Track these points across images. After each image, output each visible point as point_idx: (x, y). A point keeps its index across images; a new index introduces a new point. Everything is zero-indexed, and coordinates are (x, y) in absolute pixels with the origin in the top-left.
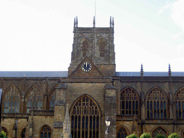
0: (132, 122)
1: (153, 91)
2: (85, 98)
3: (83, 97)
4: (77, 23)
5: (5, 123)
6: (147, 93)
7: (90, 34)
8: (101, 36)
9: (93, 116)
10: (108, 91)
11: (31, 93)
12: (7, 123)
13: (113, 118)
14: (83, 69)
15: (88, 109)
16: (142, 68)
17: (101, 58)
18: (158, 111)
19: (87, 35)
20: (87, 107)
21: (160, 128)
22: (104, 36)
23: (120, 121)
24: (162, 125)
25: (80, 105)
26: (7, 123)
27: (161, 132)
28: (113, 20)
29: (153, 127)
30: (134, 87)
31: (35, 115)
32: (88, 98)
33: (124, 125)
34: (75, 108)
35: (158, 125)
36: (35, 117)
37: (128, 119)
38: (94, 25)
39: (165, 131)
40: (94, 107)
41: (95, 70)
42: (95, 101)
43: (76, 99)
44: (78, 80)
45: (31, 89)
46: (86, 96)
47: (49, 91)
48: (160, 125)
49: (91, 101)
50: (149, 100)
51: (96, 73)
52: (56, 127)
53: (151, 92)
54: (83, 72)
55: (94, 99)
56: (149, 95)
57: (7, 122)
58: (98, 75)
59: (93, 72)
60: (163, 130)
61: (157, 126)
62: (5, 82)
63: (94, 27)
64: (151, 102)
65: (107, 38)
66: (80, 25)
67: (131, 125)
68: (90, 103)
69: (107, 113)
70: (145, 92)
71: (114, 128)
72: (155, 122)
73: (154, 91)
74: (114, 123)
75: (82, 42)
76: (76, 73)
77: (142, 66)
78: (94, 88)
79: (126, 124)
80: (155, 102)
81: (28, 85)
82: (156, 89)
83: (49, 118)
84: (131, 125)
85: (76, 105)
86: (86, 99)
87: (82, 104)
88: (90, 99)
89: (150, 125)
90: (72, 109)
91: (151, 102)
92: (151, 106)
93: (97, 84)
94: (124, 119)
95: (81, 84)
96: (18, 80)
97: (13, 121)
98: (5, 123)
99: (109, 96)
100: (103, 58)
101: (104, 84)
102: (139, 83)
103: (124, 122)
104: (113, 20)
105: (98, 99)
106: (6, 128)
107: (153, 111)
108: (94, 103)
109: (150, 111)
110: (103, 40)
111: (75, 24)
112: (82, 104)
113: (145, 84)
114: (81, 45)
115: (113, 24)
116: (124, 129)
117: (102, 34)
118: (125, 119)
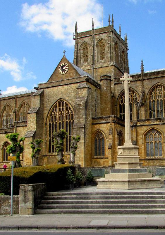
0: (109, 124)
1: (155, 89)
2: (61, 102)
3: (59, 102)
6: (148, 93)
7: (89, 38)
8: (100, 37)
9: (68, 121)
10: (80, 91)
13: (82, 122)
14: (60, 71)
15: (64, 114)
16: (142, 64)
17: (101, 60)
18: (162, 110)
19: (87, 40)
20: (63, 113)
21: (153, 130)
23: (97, 124)
24: (155, 126)
25: (56, 111)
27: (155, 134)
28: (112, 19)
29: (145, 129)
30: (133, 87)
31: (18, 127)
33: (101, 129)
34: (51, 114)
35: (151, 127)
36: (18, 128)
37: (105, 121)
38: (93, 27)
39: (160, 133)
40: (70, 112)
41: (71, 70)
42: (70, 104)
43: (52, 105)
44: (54, 84)
46: (61, 101)
48: (153, 126)
49: (67, 105)
50: (151, 99)
51: (72, 74)
52: (27, 136)
53: (153, 90)
54: (60, 75)
55: (69, 103)
56: (152, 93)
58: (75, 75)
59: (70, 73)
60: (158, 131)
61: (149, 128)
62: (18, 99)
63: (93, 29)
64: (154, 101)
65: (106, 39)
66: (79, 31)
67: (108, 128)
68: (66, 108)
69: (76, 115)
70: (147, 91)
71: (81, 132)
72: (148, 123)
73: (157, 88)
74: (82, 127)
75: (82, 48)
77: (142, 62)
78: (69, 91)
79: (103, 127)
80: (158, 100)
82: (159, 85)
84: (108, 128)
85: (53, 111)
86: (62, 104)
87: (58, 110)
88: (65, 102)
89: (142, 127)
90: (49, 117)
91: (154, 101)
92: (154, 106)
93: (72, 85)
94: (100, 122)
95: (57, 87)
96: (28, 96)
99: (81, 96)
100: (103, 61)
102: (139, 82)
103: (100, 125)
104: (112, 19)
105: (72, 102)
107: (156, 112)
108: (70, 107)
109: (152, 112)
110: (103, 41)
112: (58, 110)
113: (146, 82)
114: (82, 51)
115: (113, 22)
116: (101, 133)
117: (101, 35)
118: (102, 122)
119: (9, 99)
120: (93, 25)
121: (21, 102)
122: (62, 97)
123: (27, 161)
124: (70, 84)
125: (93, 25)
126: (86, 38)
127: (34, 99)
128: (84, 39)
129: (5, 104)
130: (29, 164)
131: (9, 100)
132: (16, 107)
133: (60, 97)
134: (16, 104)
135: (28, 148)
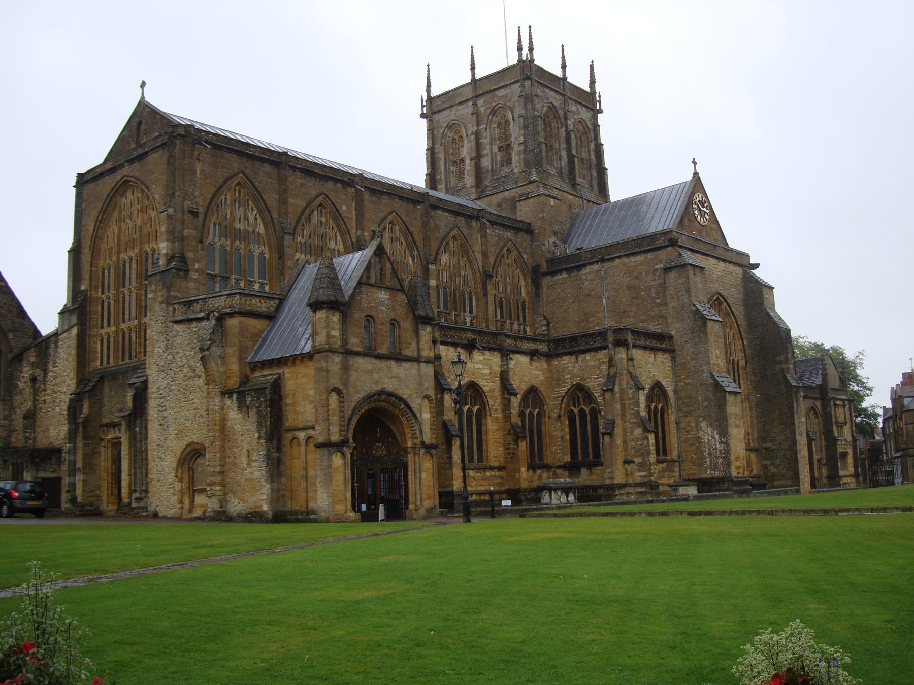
4: (531, 49)
5: (477, 366)
8: (578, 113)
11: (444, 258)
12: (481, 366)
22: (585, 114)
26: (481, 366)
32: (720, 304)
45: (444, 243)
47: (492, 260)
57: (480, 362)
62: (366, 195)
76: (686, 222)
81: (437, 227)
83: (660, 356)
93: (732, 268)
96: (408, 200)
97: (495, 359)
98: (477, 366)
101: (739, 271)
106: (481, 384)
110: (580, 127)
111: (520, 49)
119: (327, 178)
120: (564, 67)
121: (383, 214)
122: (722, 292)
123: (738, 464)
124: (730, 262)
125: (564, 67)
126: (552, 94)
127: (694, 274)
128: (547, 91)
129: (313, 193)
130: (741, 471)
131: (330, 184)
132: (360, 225)
133: (715, 287)
134: (360, 215)
135: (737, 426)
